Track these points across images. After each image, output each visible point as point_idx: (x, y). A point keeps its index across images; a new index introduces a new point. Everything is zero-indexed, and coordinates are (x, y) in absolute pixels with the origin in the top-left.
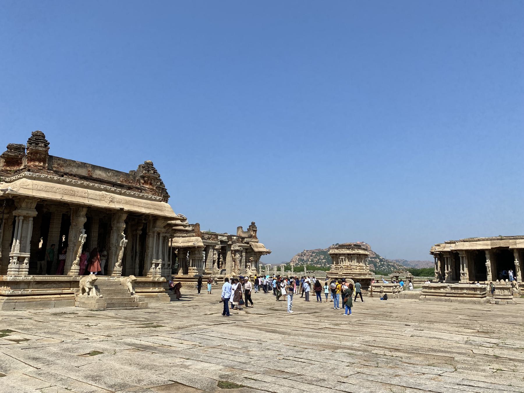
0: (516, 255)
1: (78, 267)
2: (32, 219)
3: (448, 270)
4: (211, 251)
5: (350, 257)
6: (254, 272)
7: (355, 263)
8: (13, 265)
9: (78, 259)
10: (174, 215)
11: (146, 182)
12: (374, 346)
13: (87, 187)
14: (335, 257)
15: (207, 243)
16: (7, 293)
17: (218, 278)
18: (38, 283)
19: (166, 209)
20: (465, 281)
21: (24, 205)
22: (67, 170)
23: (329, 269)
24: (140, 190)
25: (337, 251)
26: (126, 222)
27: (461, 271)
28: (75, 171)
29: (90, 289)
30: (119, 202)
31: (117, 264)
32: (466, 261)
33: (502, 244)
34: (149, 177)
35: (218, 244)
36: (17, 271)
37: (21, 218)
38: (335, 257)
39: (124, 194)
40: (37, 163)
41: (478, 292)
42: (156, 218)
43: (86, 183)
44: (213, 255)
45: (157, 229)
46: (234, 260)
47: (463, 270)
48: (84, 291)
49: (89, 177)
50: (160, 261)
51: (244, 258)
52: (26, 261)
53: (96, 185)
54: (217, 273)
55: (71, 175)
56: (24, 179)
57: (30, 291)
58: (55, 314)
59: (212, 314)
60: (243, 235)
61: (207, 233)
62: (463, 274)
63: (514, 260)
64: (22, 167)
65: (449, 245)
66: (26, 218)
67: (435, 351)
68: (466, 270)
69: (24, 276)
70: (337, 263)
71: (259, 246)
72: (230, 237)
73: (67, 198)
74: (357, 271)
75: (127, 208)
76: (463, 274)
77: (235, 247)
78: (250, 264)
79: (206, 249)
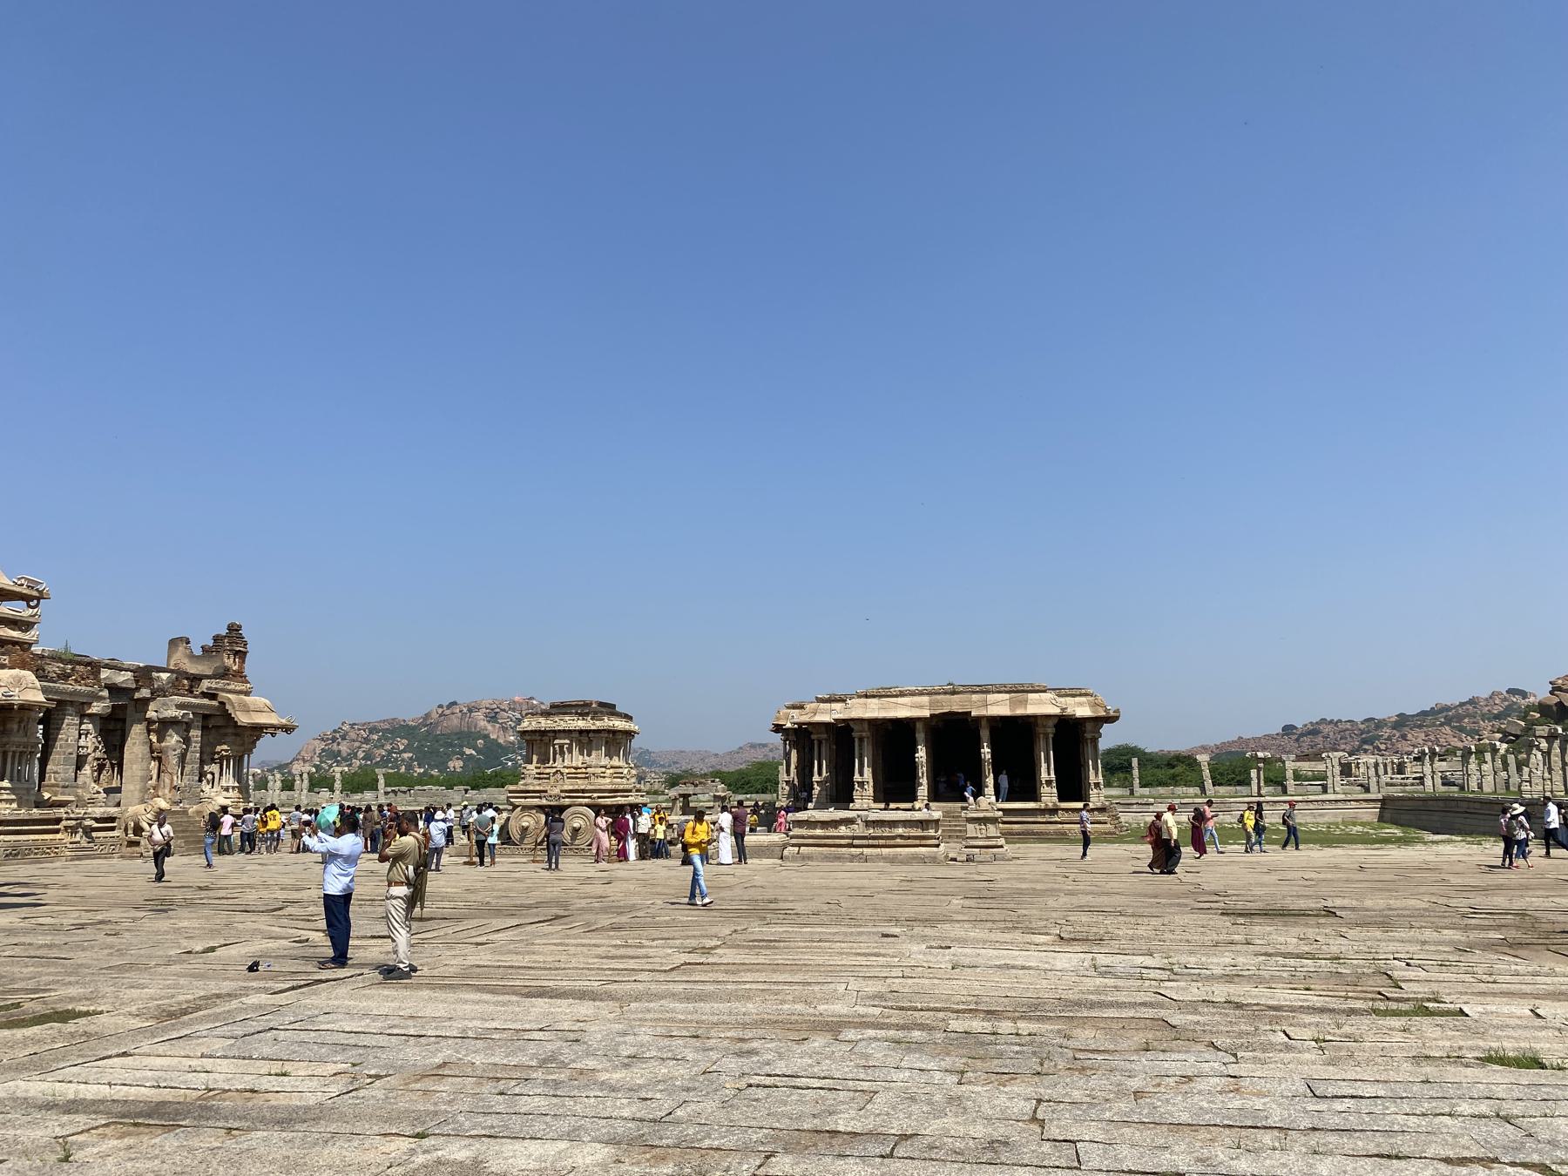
0: (985, 734)
3: (820, 774)
5: (585, 739)
6: (231, 793)
7: (598, 758)
12: (916, 1009)
14: (539, 743)
15: (57, 692)
17: (97, 820)
20: (864, 801)
23: (517, 776)
25: (545, 723)
27: (857, 777)
32: (868, 749)
33: (955, 704)
35: (101, 698)
38: (539, 743)
41: (932, 832)
44: (79, 737)
46: (157, 756)
47: (861, 774)
51: (196, 746)
54: (92, 801)
59: (213, 949)
60: (193, 669)
61: (55, 657)
62: (861, 784)
63: (980, 747)
65: (827, 705)
67: (1092, 1005)
68: (868, 772)
70: (544, 760)
71: (252, 708)
72: (144, 675)
74: (606, 783)
76: (861, 784)
77: (166, 708)
78: (215, 768)
79: (51, 719)
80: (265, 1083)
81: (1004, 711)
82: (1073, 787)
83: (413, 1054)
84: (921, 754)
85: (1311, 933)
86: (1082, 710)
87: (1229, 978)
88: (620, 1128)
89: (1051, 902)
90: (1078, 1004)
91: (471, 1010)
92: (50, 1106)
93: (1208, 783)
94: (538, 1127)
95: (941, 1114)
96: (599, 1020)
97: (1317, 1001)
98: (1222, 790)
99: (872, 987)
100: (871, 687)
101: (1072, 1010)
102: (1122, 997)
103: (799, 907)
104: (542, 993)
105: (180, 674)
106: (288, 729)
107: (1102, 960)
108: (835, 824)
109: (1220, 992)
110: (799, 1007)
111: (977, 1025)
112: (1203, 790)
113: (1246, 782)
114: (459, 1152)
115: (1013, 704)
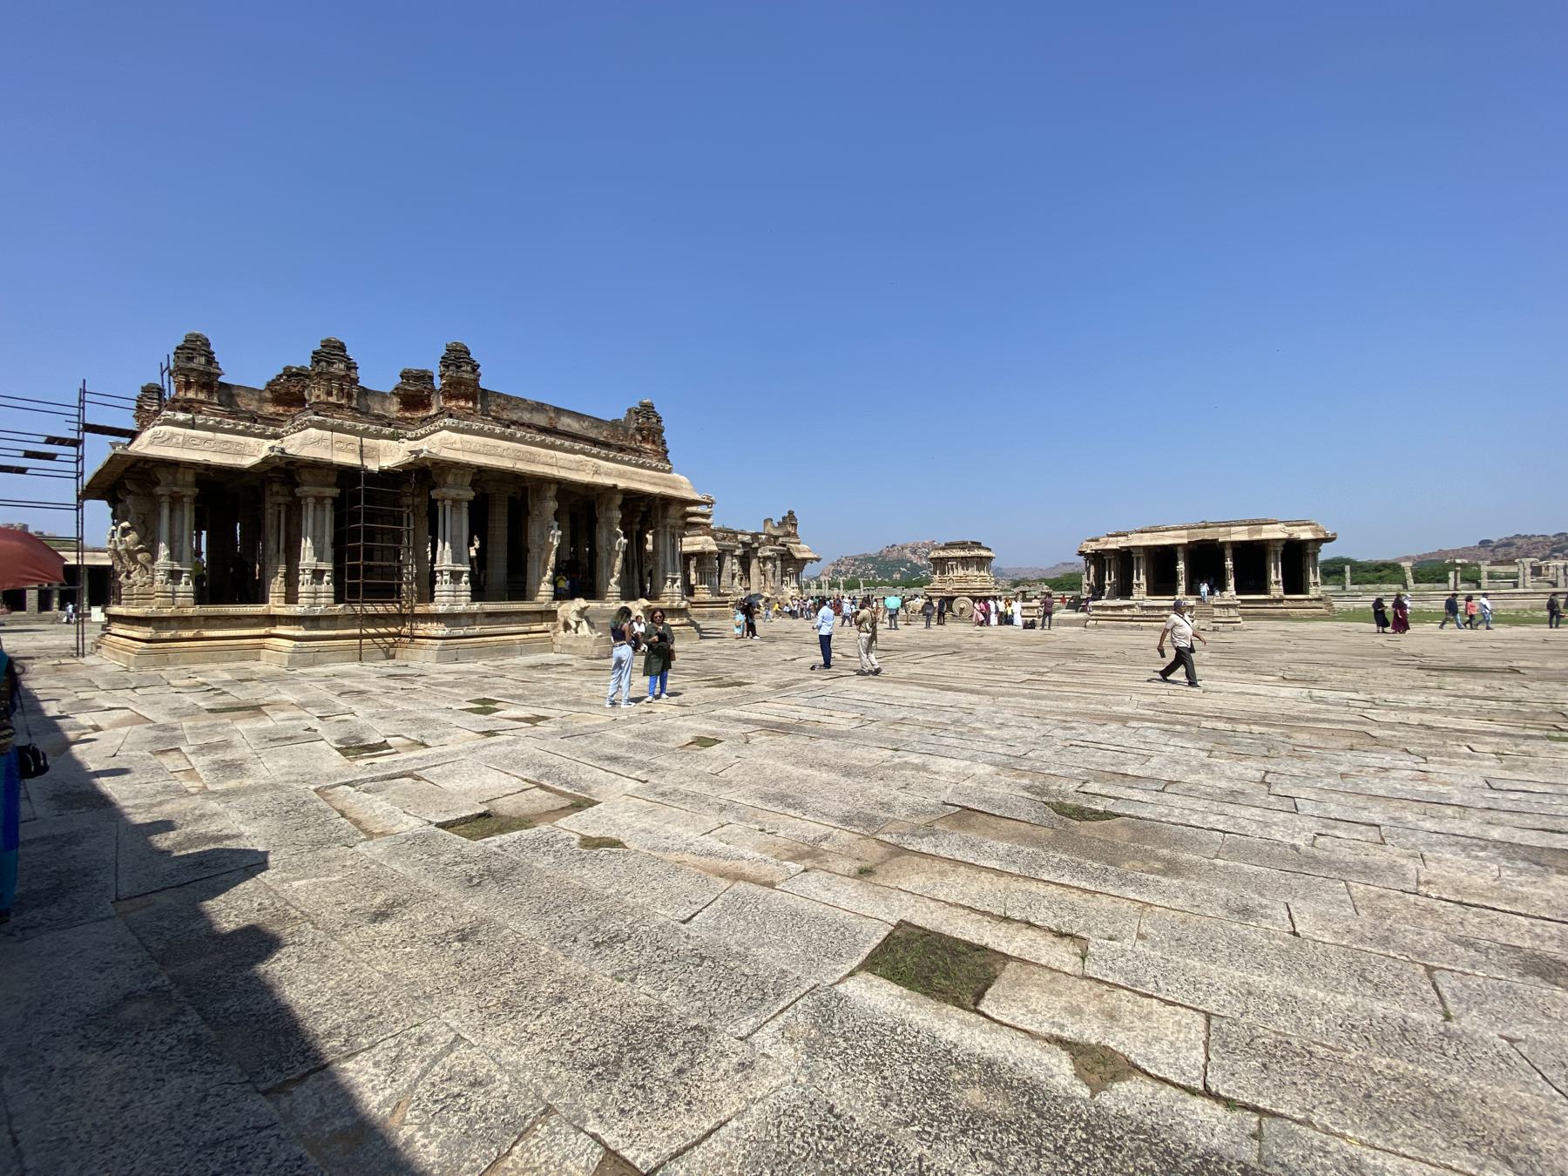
0: (1228, 553)
1: (551, 587)
2: (466, 504)
4: (728, 558)
7: (972, 572)
8: (443, 587)
9: (550, 573)
10: (697, 497)
11: (644, 439)
13: (552, 447)
14: (940, 564)
16: (441, 633)
18: (489, 615)
19: (679, 484)
20: (1140, 595)
21: (450, 479)
22: (515, 417)
24: (638, 452)
25: (942, 554)
26: (621, 508)
28: (526, 417)
29: (578, 623)
30: (608, 474)
31: (612, 581)
32: (1143, 564)
33: (1207, 535)
34: (649, 429)
36: (451, 596)
37: (448, 503)
38: (940, 564)
39: (613, 460)
40: (462, 403)
42: (667, 501)
43: (549, 439)
44: (731, 565)
45: (671, 521)
46: (763, 573)
48: (567, 626)
49: (550, 427)
50: (678, 575)
52: (465, 578)
53: (567, 443)
55: (523, 425)
56: (445, 433)
57: (477, 629)
58: (534, 667)
60: (775, 533)
61: (720, 530)
63: (1223, 560)
64: (433, 412)
66: (456, 502)
67: (1308, 720)
68: (1143, 579)
69: (464, 605)
70: (943, 573)
71: (802, 550)
72: (755, 536)
73: (522, 466)
74: (977, 585)
75: (622, 484)
77: (765, 552)
80: (823, 719)
81: (1244, 537)
82: (1295, 584)
83: (889, 713)
84: (1181, 566)
85: (1496, 683)
86: (1305, 534)
87: (1422, 710)
88: (998, 758)
89: (1277, 657)
90: (1298, 718)
91: (914, 694)
92: (739, 720)
93: (1410, 582)
94: (954, 753)
95: (1197, 772)
96: (983, 705)
97: (1500, 729)
98: (1422, 586)
99: (1148, 699)
100: (1144, 527)
101: (1291, 722)
102: (1332, 716)
103: (1097, 654)
104: (950, 689)
105: (770, 535)
106: (818, 560)
107: (1316, 693)
108: (1121, 608)
109: (1414, 718)
110: (1100, 707)
111: (1221, 725)
112: (1406, 587)
113: (1446, 580)
114: (915, 759)
115: (1250, 532)
